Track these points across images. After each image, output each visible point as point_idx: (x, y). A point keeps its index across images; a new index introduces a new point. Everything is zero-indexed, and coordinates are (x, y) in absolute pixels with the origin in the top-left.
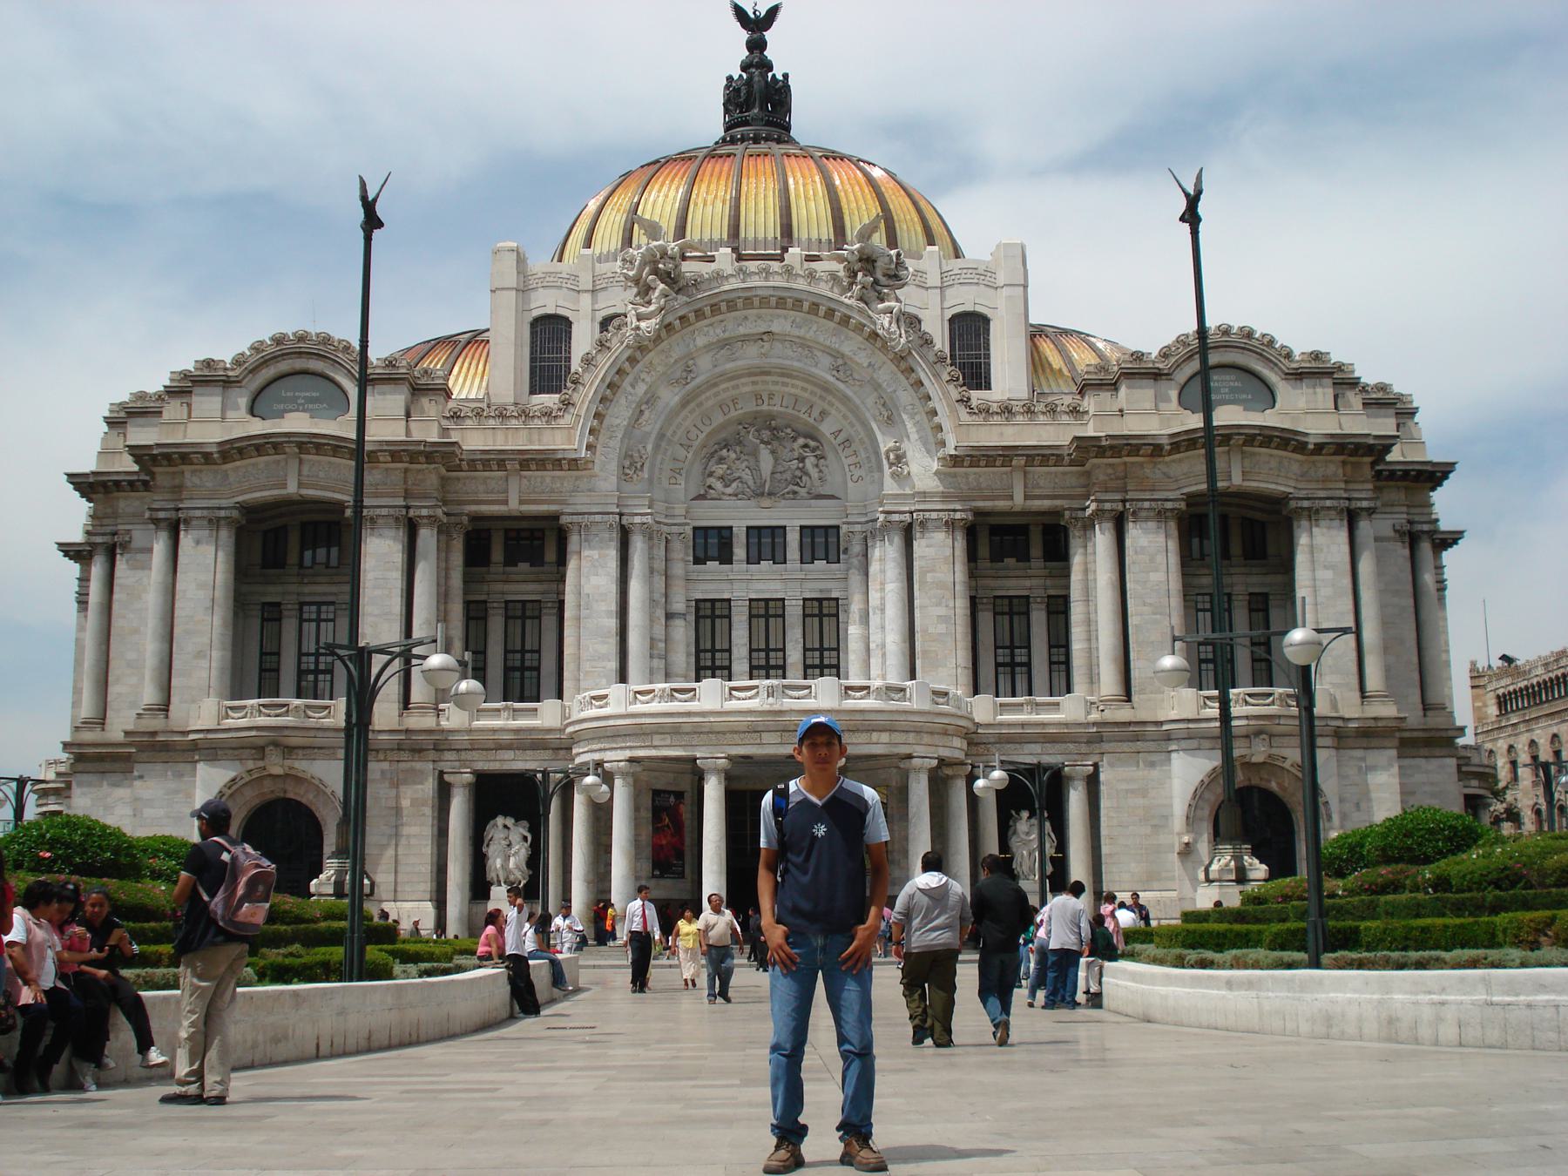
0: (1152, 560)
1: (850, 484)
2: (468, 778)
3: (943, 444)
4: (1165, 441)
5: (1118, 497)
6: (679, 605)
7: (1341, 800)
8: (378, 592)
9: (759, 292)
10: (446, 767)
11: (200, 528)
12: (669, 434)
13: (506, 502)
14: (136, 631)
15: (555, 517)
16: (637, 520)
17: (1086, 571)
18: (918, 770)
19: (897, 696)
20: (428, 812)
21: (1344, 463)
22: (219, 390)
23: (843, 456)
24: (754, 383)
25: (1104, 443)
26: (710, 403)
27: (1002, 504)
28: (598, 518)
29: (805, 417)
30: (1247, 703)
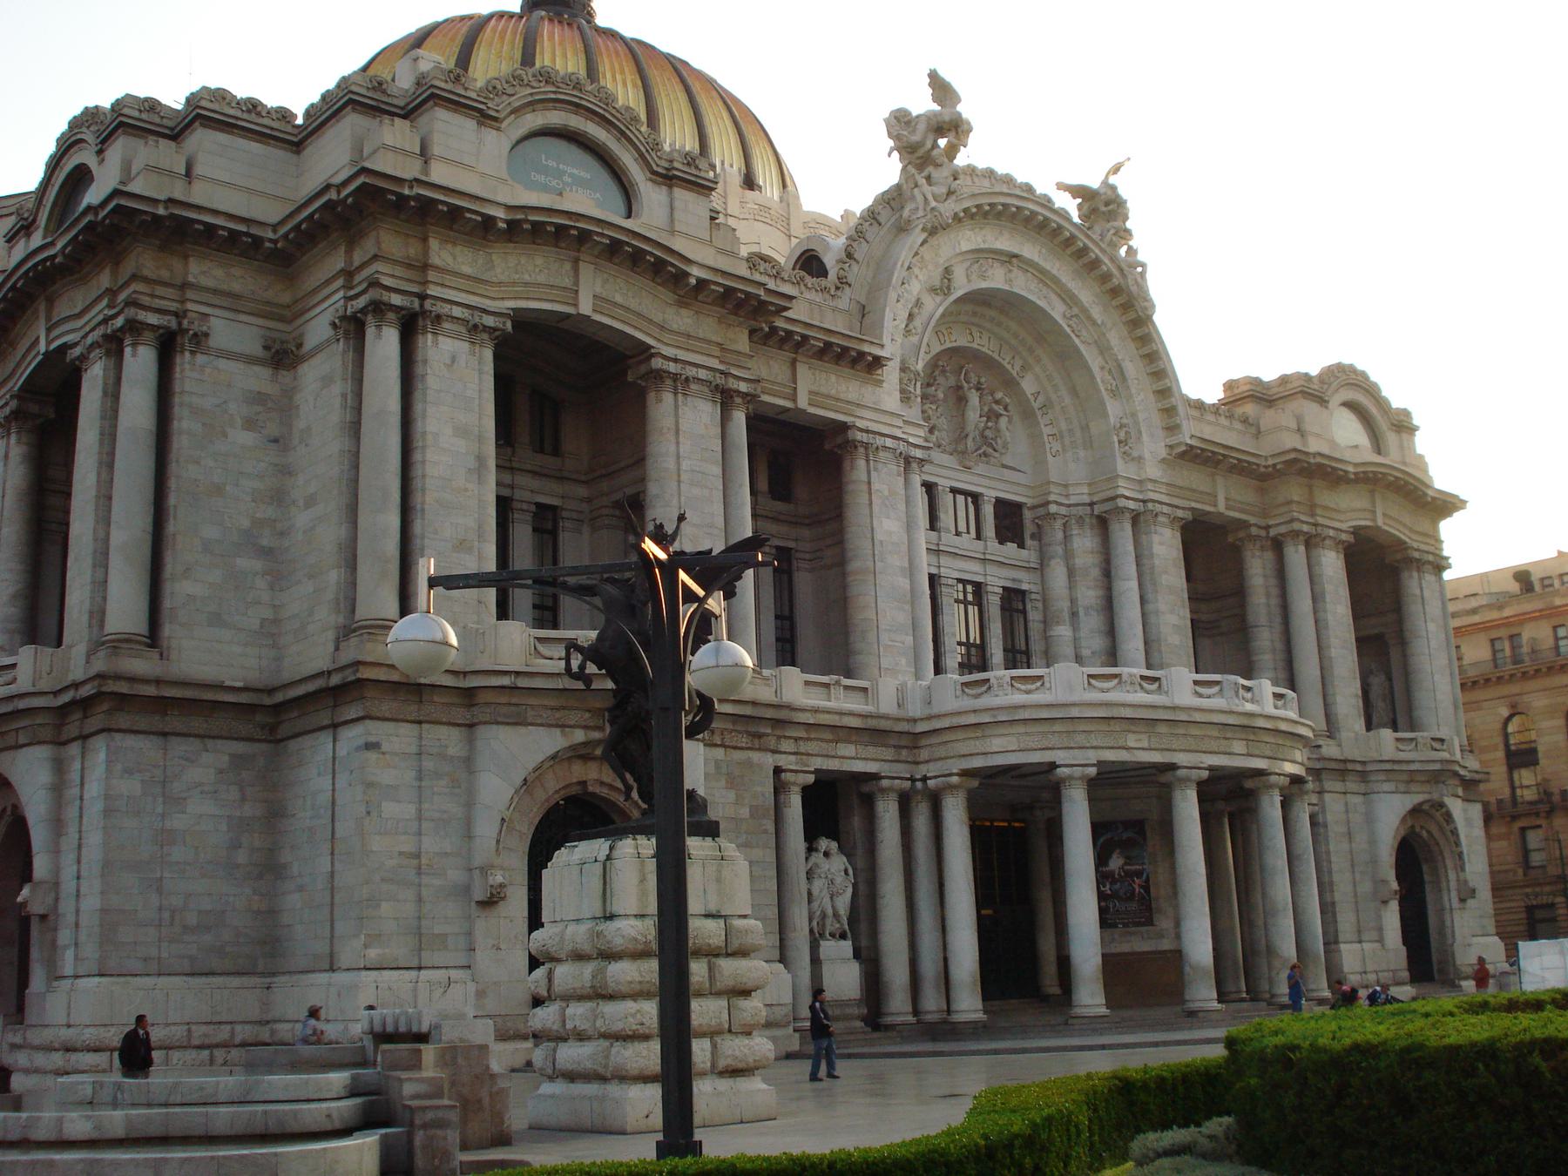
1: (1049, 457)
2: (811, 779)
3: (1172, 429)
8: (696, 491)
10: (785, 761)
11: (457, 337)
13: (793, 397)
14: (218, 490)
15: (843, 427)
17: (1268, 595)
20: (771, 827)
22: (470, 124)
23: (1042, 421)
24: (975, 314)
28: (889, 442)
29: (1009, 367)
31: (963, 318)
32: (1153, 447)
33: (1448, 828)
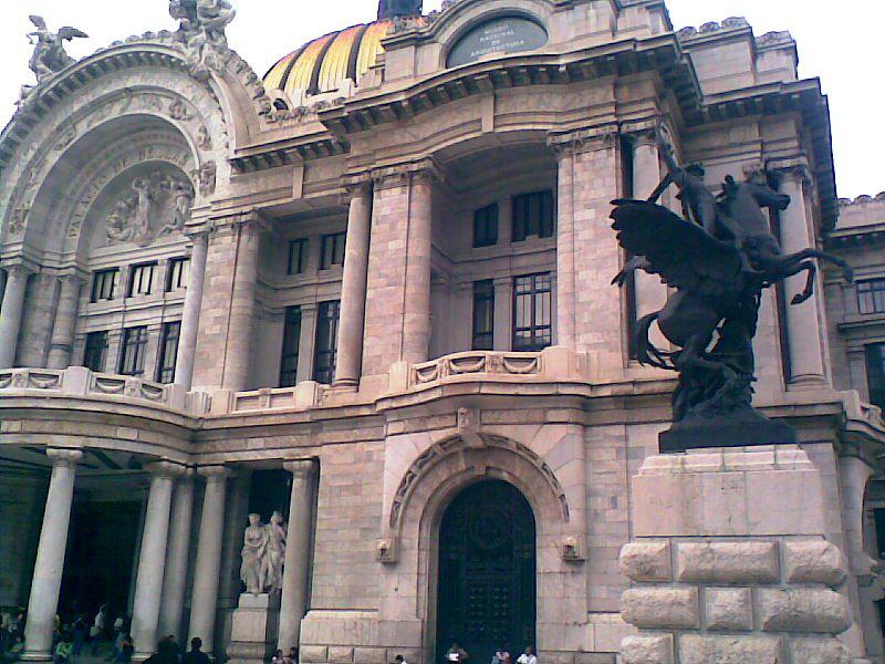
0: (393, 226)
4: (402, 97)
5: (365, 169)
6: (60, 336)
7: (588, 494)
9: (108, 55)
12: (68, 193)
16: (10, 263)
18: (59, 458)
19: (43, 383)
21: (616, 86)
24: (134, 140)
25: (345, 114)
26: (104, 164)
27: (283, 201)
30: (452, 372)
31: (131, 146)
32: (224, 172)
33: (538, 464)
